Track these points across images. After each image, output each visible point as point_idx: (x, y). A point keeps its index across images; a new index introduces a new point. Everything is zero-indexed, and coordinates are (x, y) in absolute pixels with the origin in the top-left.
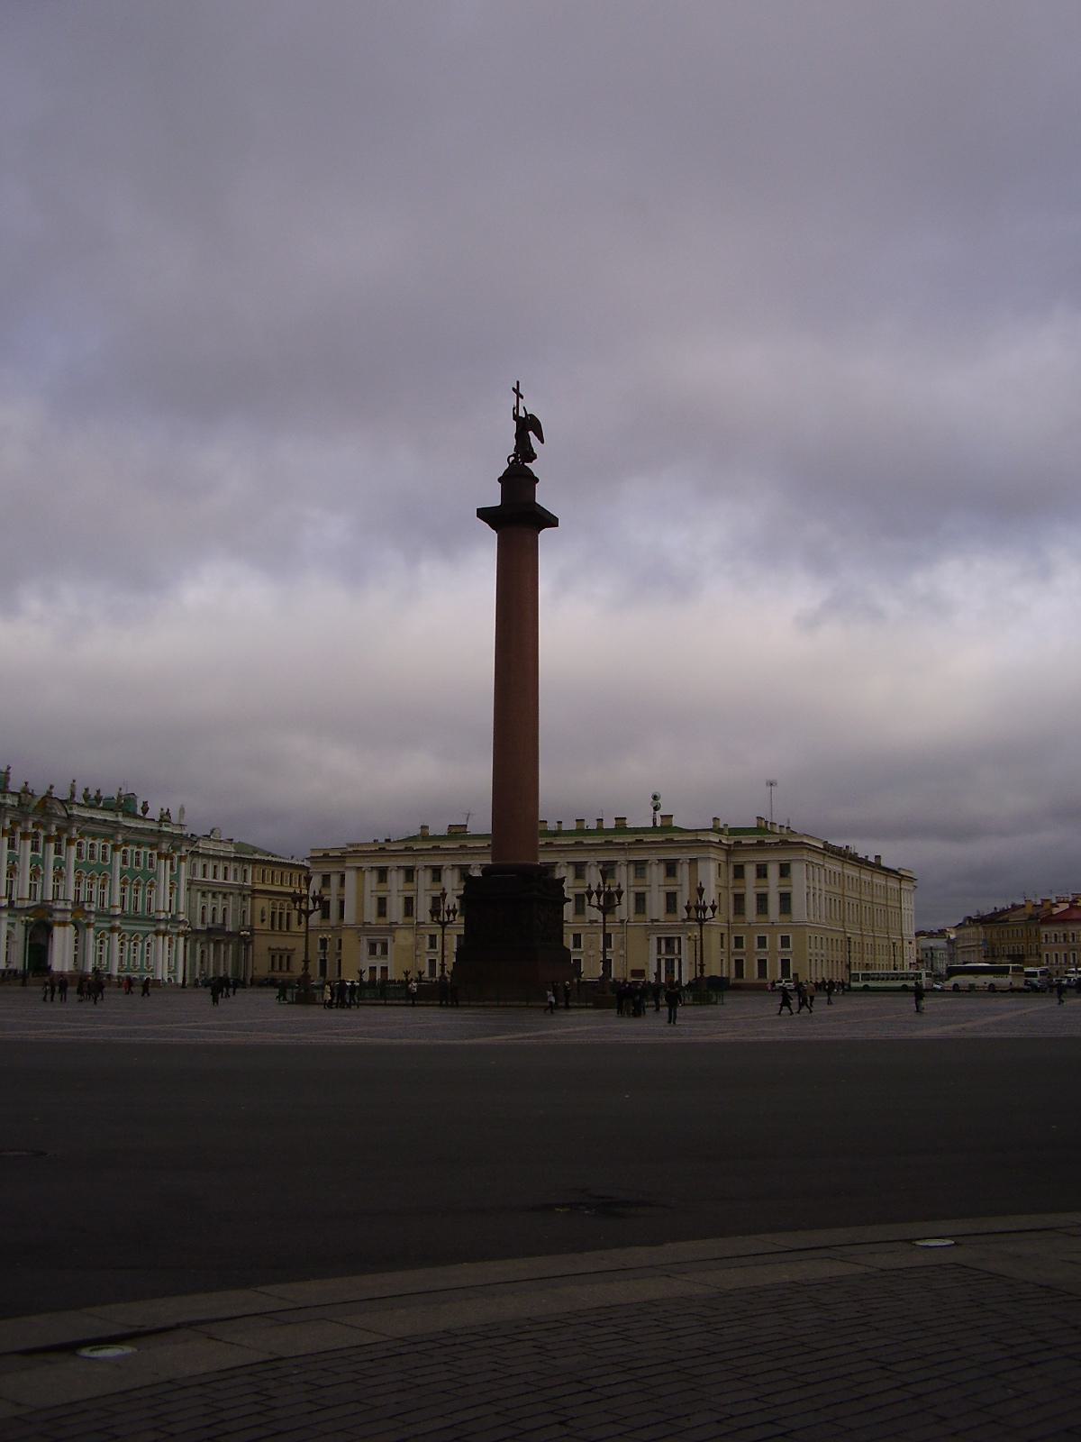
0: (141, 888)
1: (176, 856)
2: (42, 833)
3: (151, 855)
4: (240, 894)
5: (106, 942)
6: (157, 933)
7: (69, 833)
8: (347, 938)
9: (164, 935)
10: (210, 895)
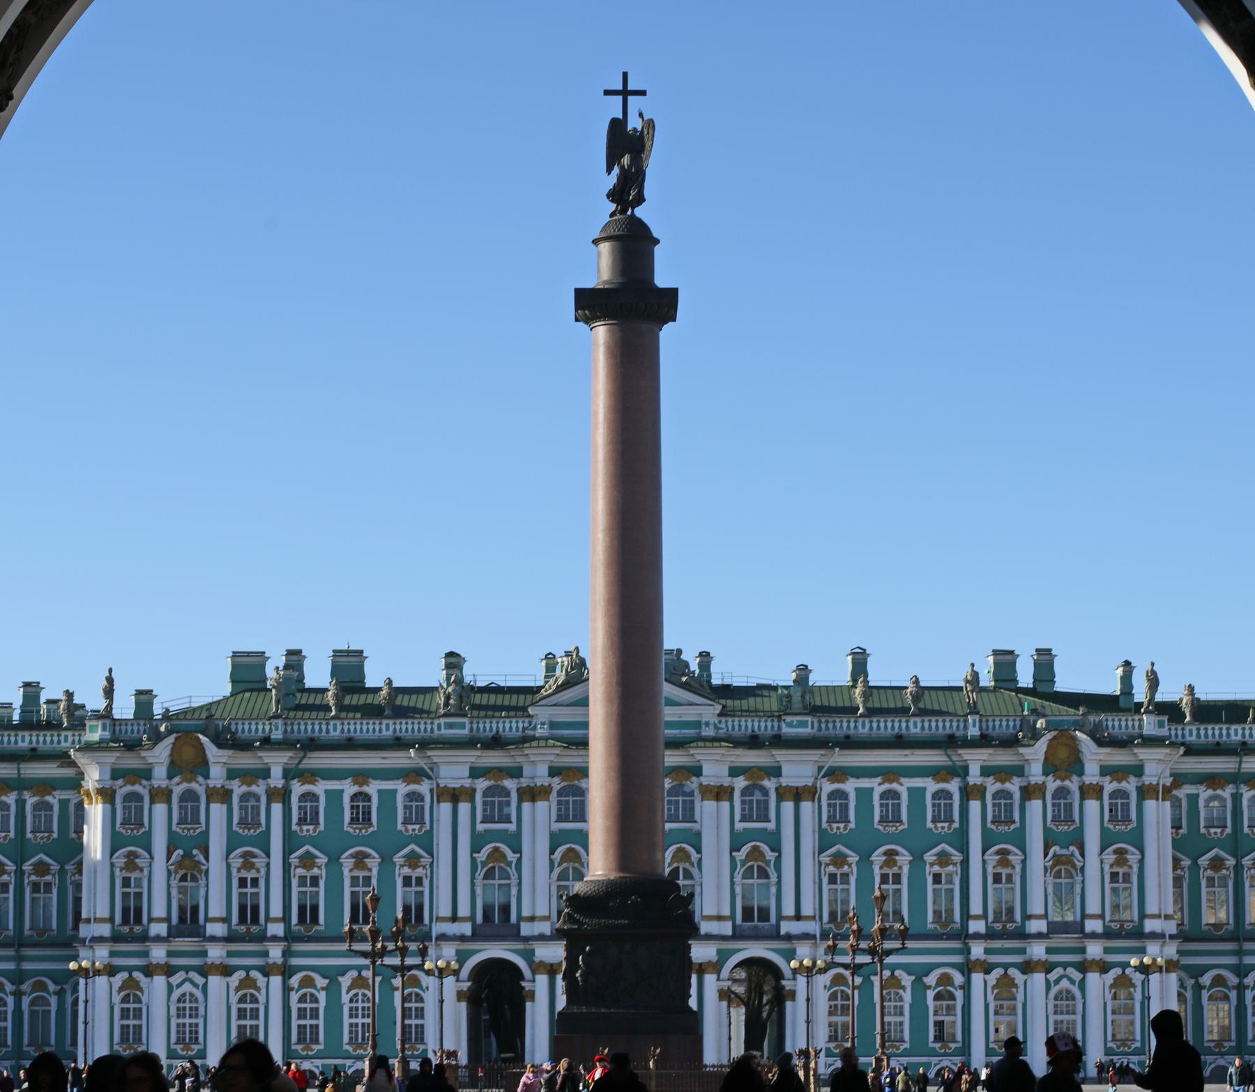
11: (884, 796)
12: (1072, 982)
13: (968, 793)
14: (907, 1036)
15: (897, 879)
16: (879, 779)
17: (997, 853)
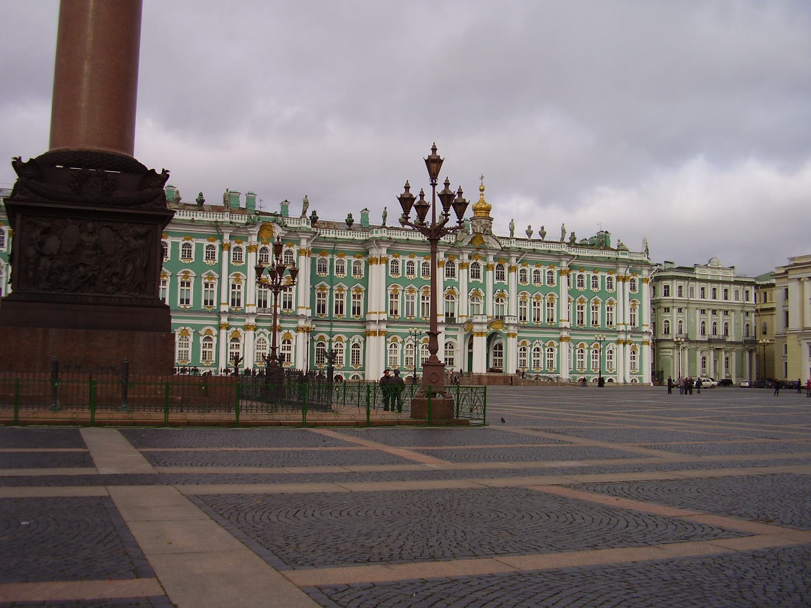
0: (599, 306)
1: (637, 278)
2: (482, 264)
3: (609, 279)
4: (742, 311)
5: (556, 349)
6: (618, 342)
7: (509, 263)
8: (791, 342)
9: (624, 344)
10: (710, 313)
11: (184, 246)
12: (266, 335)
13: (222, 247)
14: (190, 358)
15: (188, 284)
16: (182, 238)
17: (234, 275)
